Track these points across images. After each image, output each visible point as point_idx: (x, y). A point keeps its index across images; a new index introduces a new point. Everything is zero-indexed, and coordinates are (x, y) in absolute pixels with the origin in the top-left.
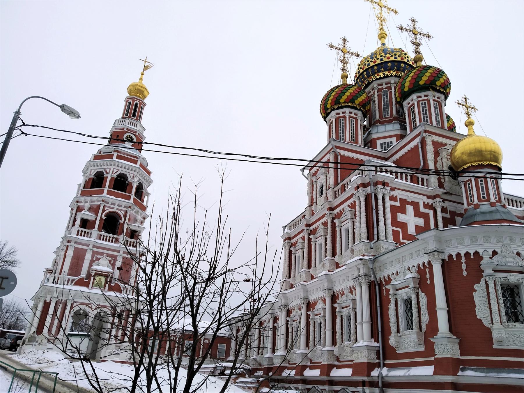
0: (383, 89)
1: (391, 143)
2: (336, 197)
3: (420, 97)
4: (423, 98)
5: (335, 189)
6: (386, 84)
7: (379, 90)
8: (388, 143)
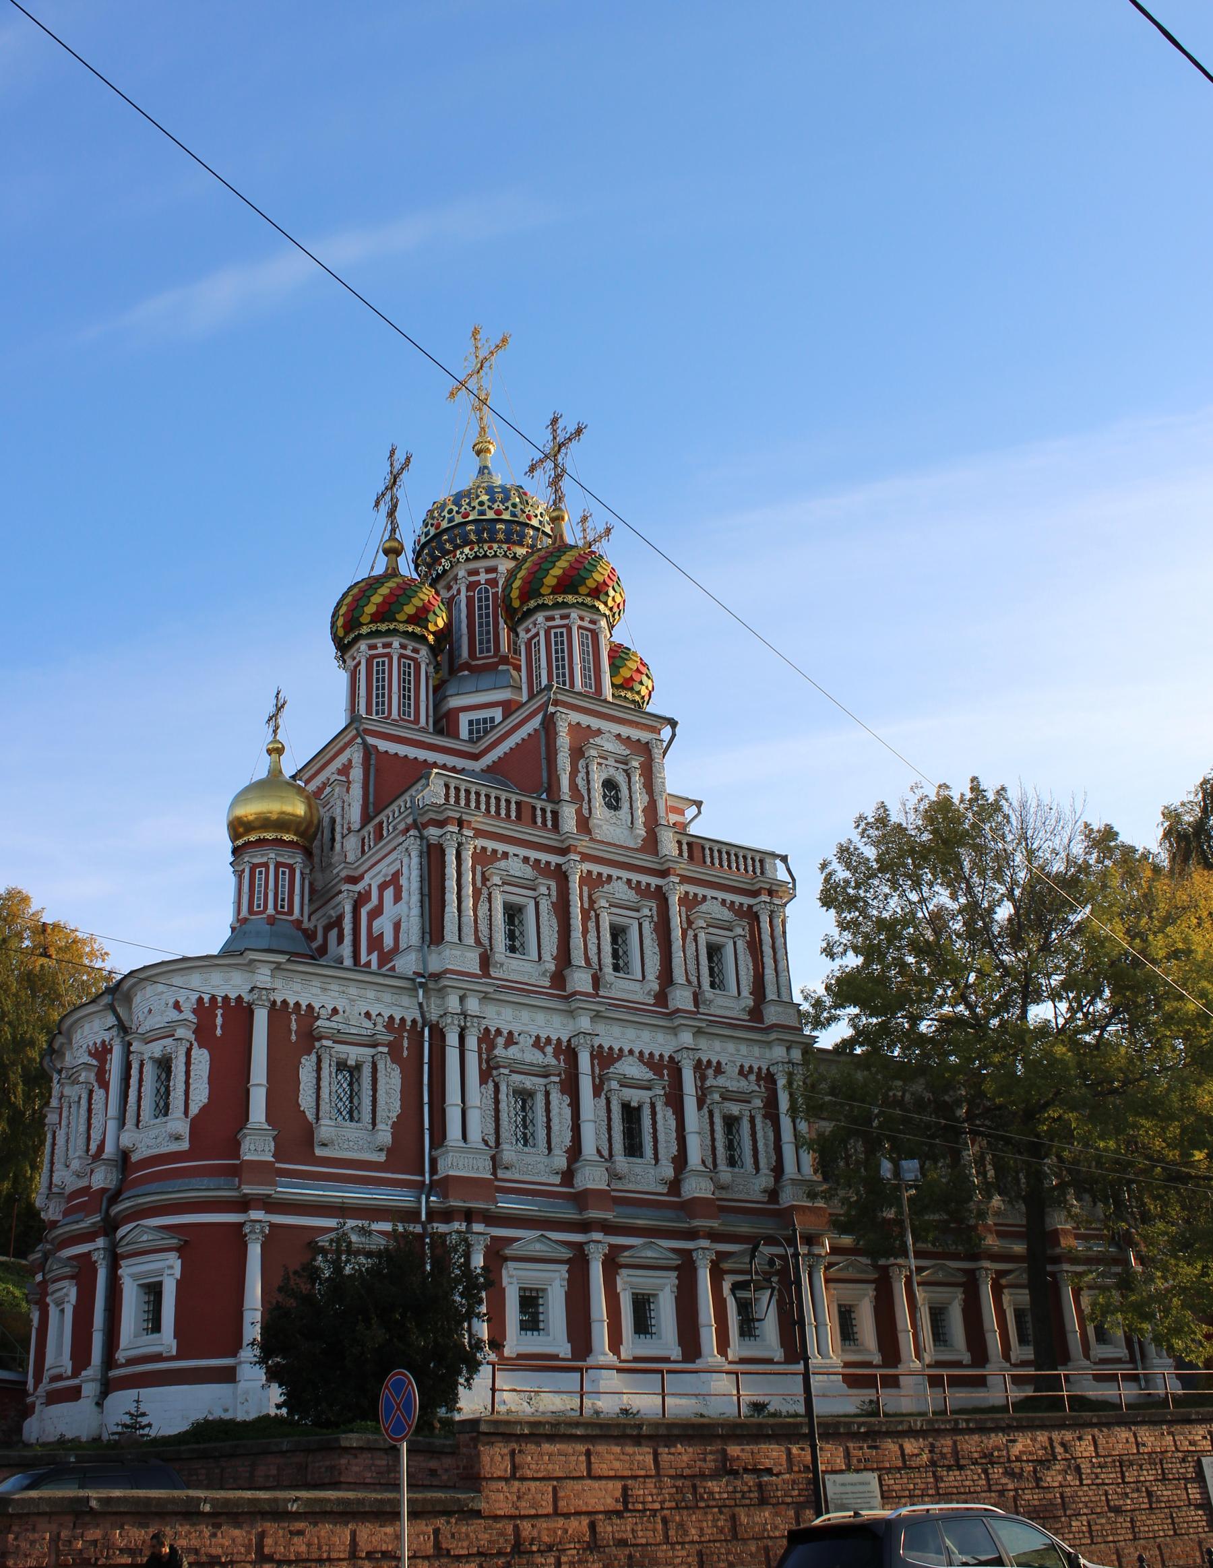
0: (478, 583)
1: (492, 719)
2: (363, 852)
3: (552, 619)
4: (558, 622)
5: (364, 832)
6: (489, 570)
7: (471, 587)
8: (485, 720)
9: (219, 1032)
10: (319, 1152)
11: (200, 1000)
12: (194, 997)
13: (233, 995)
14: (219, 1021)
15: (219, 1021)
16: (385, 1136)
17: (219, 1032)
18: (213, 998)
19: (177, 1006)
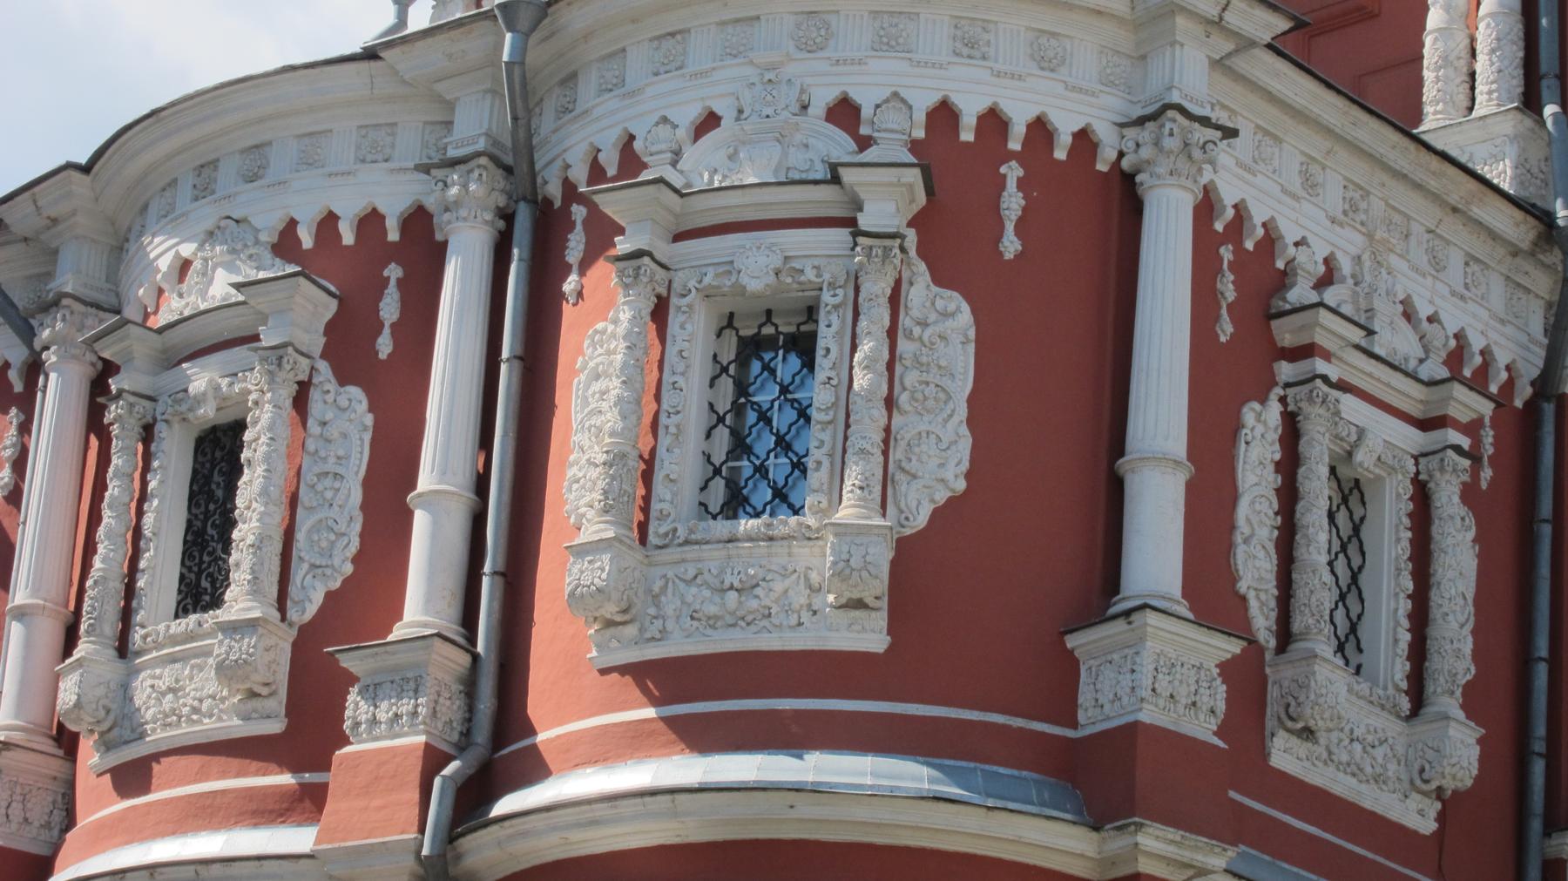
9: (1011, 245)
10: (1286, 755)
11: (944, 115)
12: (923, 102)
13: (1065, 127)
14: (1013, 203)
15: (1013, 203)
16: (1461, 750)
17: (1011, 245)
18: (994, 122)
19: (844, 113)
